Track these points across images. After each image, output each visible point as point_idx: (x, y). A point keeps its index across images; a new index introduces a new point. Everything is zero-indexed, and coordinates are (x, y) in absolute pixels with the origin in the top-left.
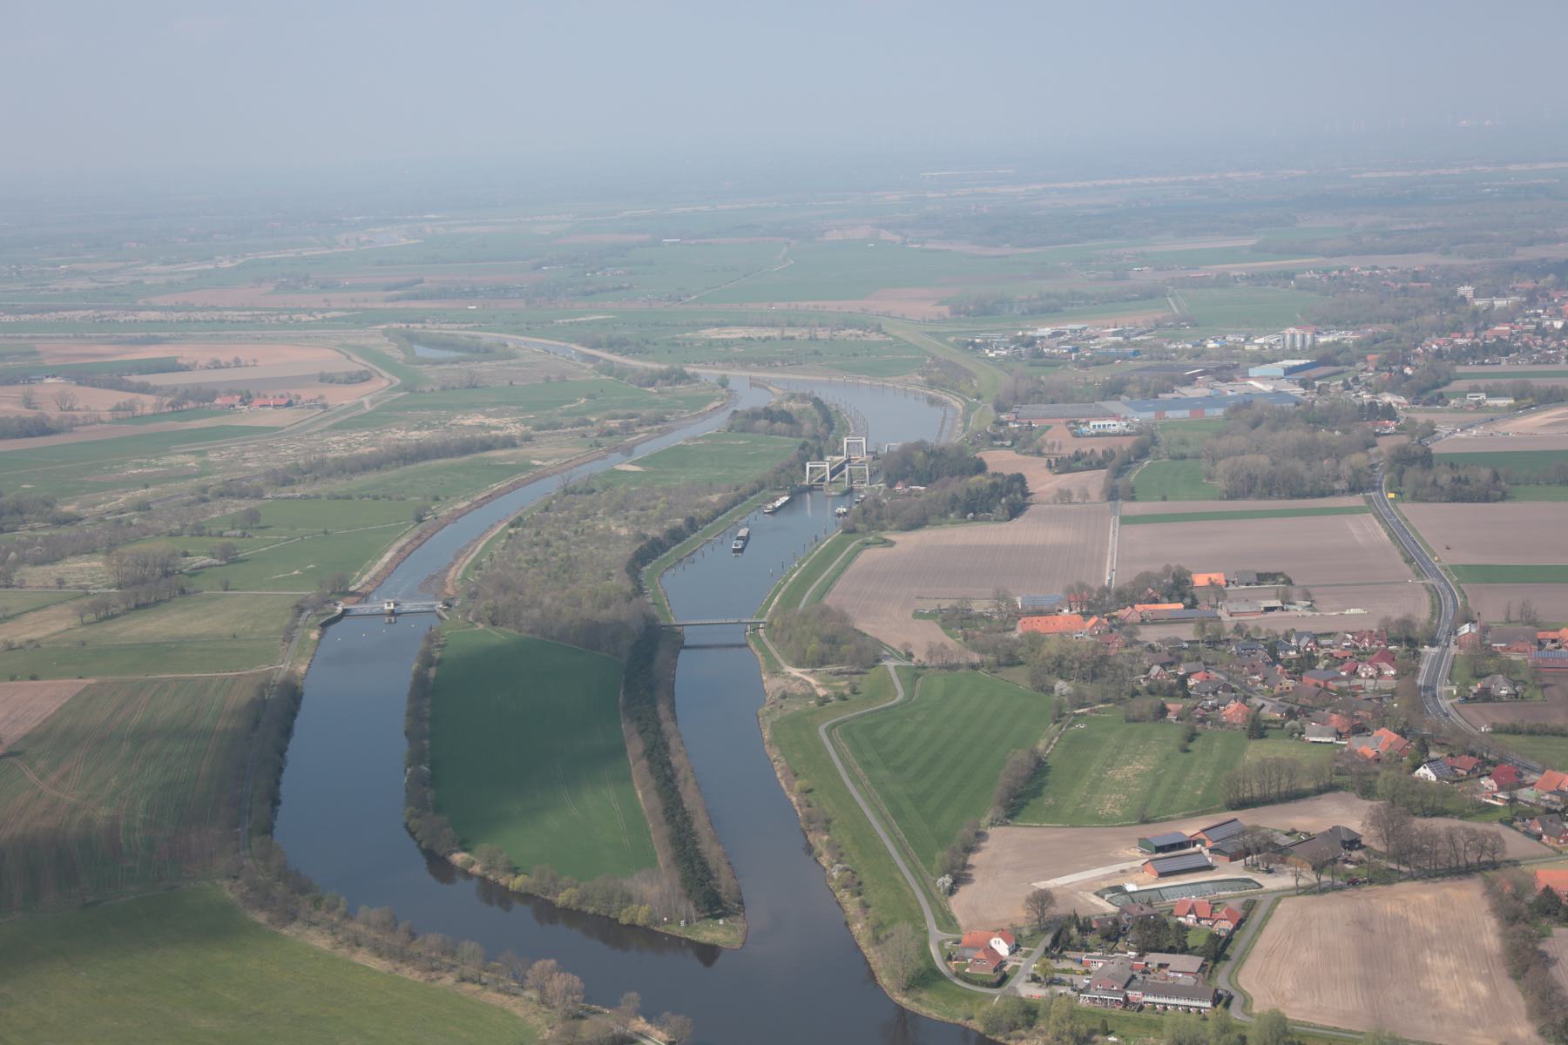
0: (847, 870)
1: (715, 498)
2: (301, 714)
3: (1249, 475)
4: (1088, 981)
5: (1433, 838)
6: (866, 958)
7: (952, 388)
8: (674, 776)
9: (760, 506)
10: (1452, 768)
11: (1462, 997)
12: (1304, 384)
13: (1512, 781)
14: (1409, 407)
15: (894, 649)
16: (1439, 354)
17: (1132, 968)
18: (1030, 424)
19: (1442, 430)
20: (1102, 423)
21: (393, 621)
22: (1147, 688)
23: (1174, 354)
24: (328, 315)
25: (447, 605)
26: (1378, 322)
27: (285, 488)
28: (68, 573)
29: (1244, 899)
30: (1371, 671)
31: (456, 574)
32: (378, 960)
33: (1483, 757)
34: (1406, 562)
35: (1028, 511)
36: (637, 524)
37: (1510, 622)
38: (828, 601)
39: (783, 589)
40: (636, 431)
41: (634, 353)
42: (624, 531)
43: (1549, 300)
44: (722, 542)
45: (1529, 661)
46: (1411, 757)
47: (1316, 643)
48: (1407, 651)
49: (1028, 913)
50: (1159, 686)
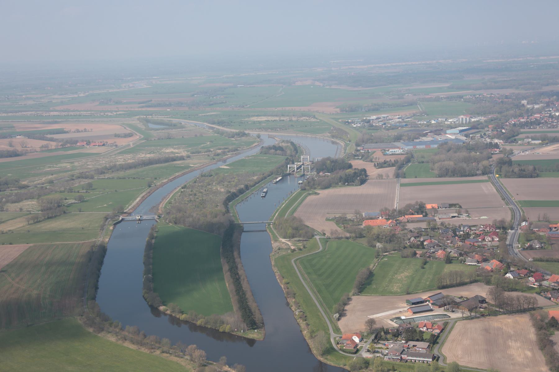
0: (301, 312)
1: (255, 178)
2: (106, 256)
3: (446, 169)
4: (388, 352)
5: (512, 299)
6: (308, 343)
7: (340, 138)
8: (239, 278)
9: (271, 181)
10: (519, 274)
11: (522, 357)
12: (466, 136)
13: (540, 279)
14: (504, 144)
15: (319, 232)
16: (514, 125)
17: (403, 347)
18: (368, 150)
19: (516, 152)
20: (394, 150)
21: (140, 223)
22: (409, 245)
23: (420, 125)
24: (118, 113)
25: (159, 217)
26: (493, 114)
27: (100, 175)
28: (24, 206)
29: (444, 322)
30: (490, 239)
31: (162, 205)
32: (133, 345)
33: (530, 270)
34: (503, 199)
35: (367, 182)
36: (227, 187)
38: (295, 215)
39: (279, 211)
40: (227, 154)
41: (227, 126)
42: (222, 190)
43: (554, 105)
44: (258, 194)
45: (546, 235)
46: (504, 270)
47: (470, 229)
48: (503, 232)
49: (366, 327)
50: (414, 245)
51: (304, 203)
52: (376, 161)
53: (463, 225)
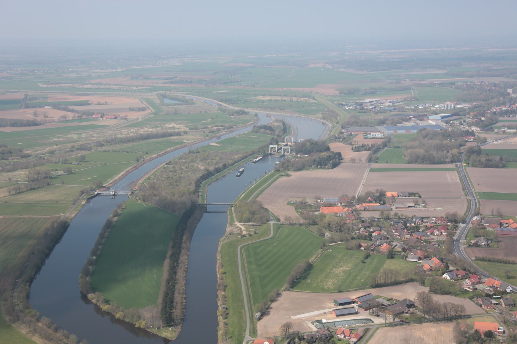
1: (236, 157)
7: (330, 120)
18: (351, 133)
34: (463, 190)
35: (339, 166)
36: (208, 165)
37: (493, 215)
39: (247, 192)
47: (422, 221)
51: (273, 184)
52: (356, 145)
53: (416, 216)
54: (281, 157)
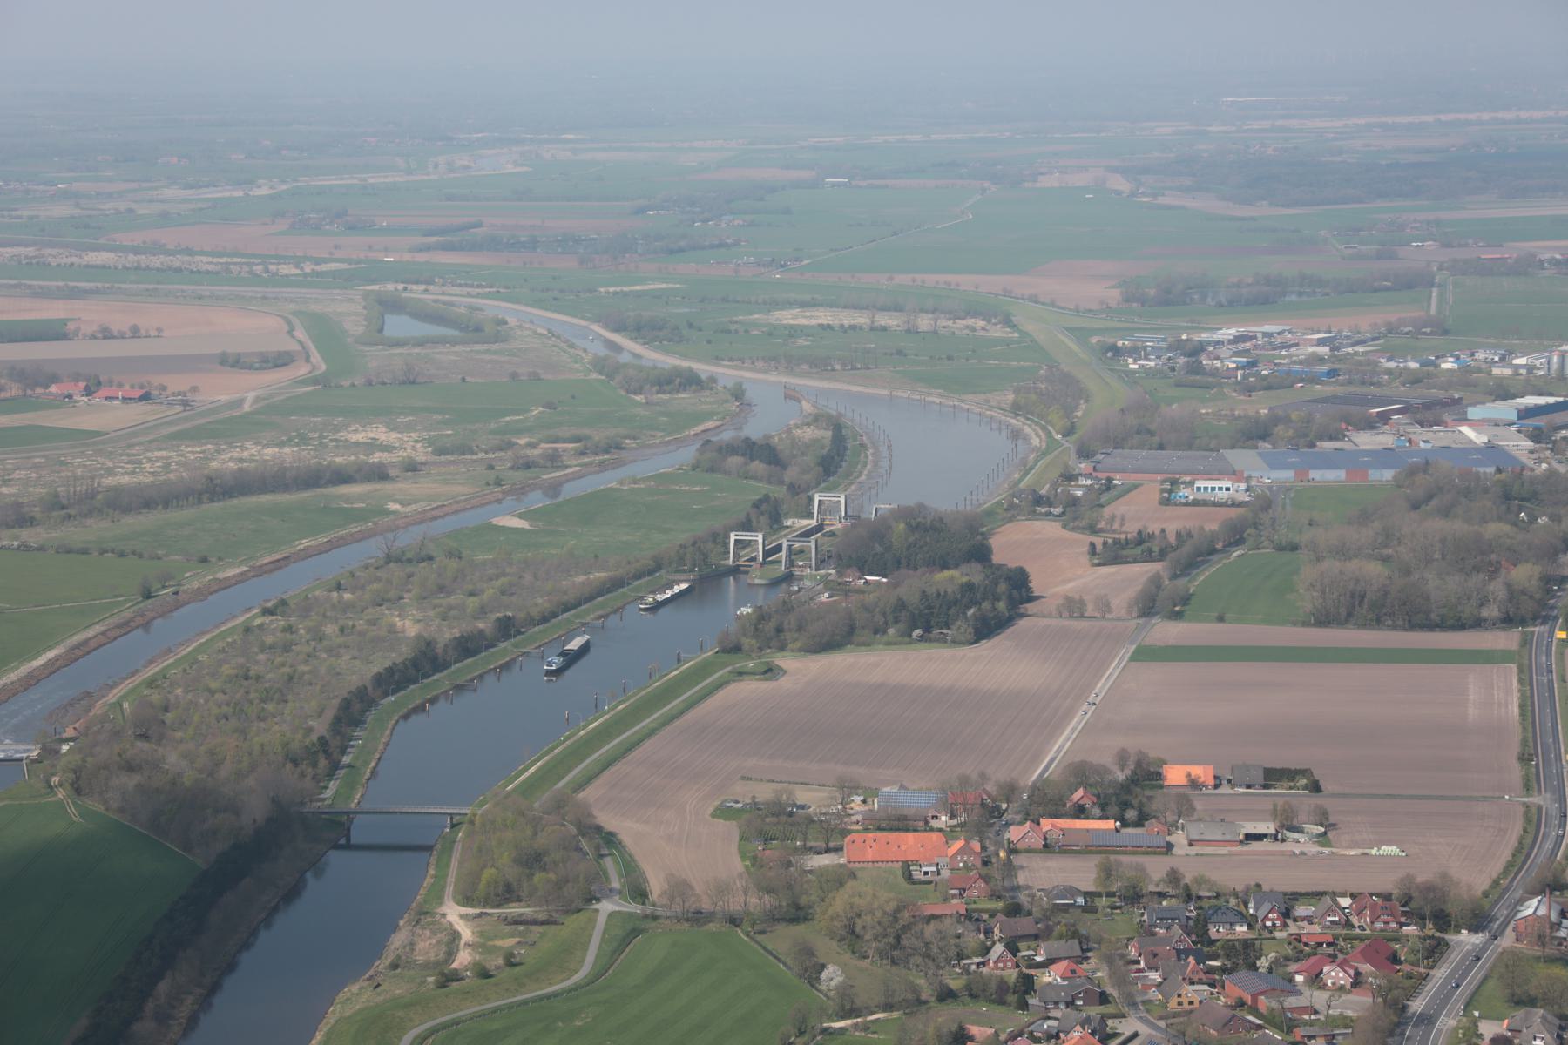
54: (775, 583)
